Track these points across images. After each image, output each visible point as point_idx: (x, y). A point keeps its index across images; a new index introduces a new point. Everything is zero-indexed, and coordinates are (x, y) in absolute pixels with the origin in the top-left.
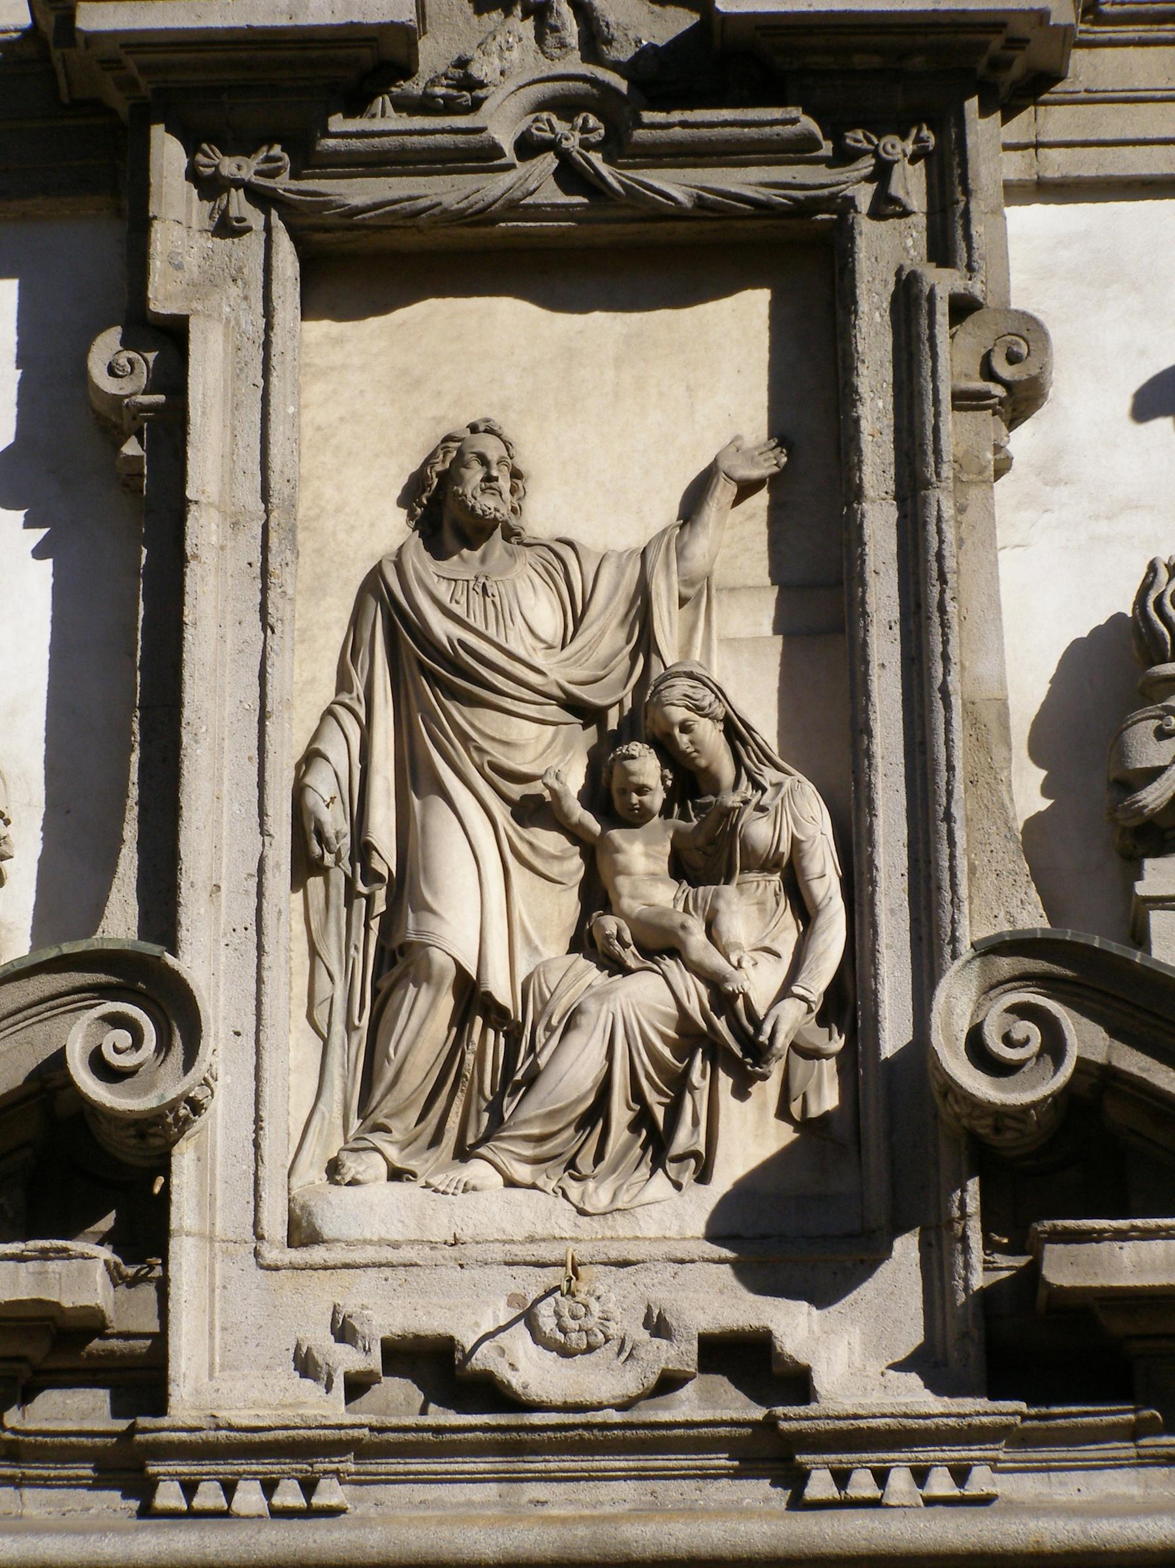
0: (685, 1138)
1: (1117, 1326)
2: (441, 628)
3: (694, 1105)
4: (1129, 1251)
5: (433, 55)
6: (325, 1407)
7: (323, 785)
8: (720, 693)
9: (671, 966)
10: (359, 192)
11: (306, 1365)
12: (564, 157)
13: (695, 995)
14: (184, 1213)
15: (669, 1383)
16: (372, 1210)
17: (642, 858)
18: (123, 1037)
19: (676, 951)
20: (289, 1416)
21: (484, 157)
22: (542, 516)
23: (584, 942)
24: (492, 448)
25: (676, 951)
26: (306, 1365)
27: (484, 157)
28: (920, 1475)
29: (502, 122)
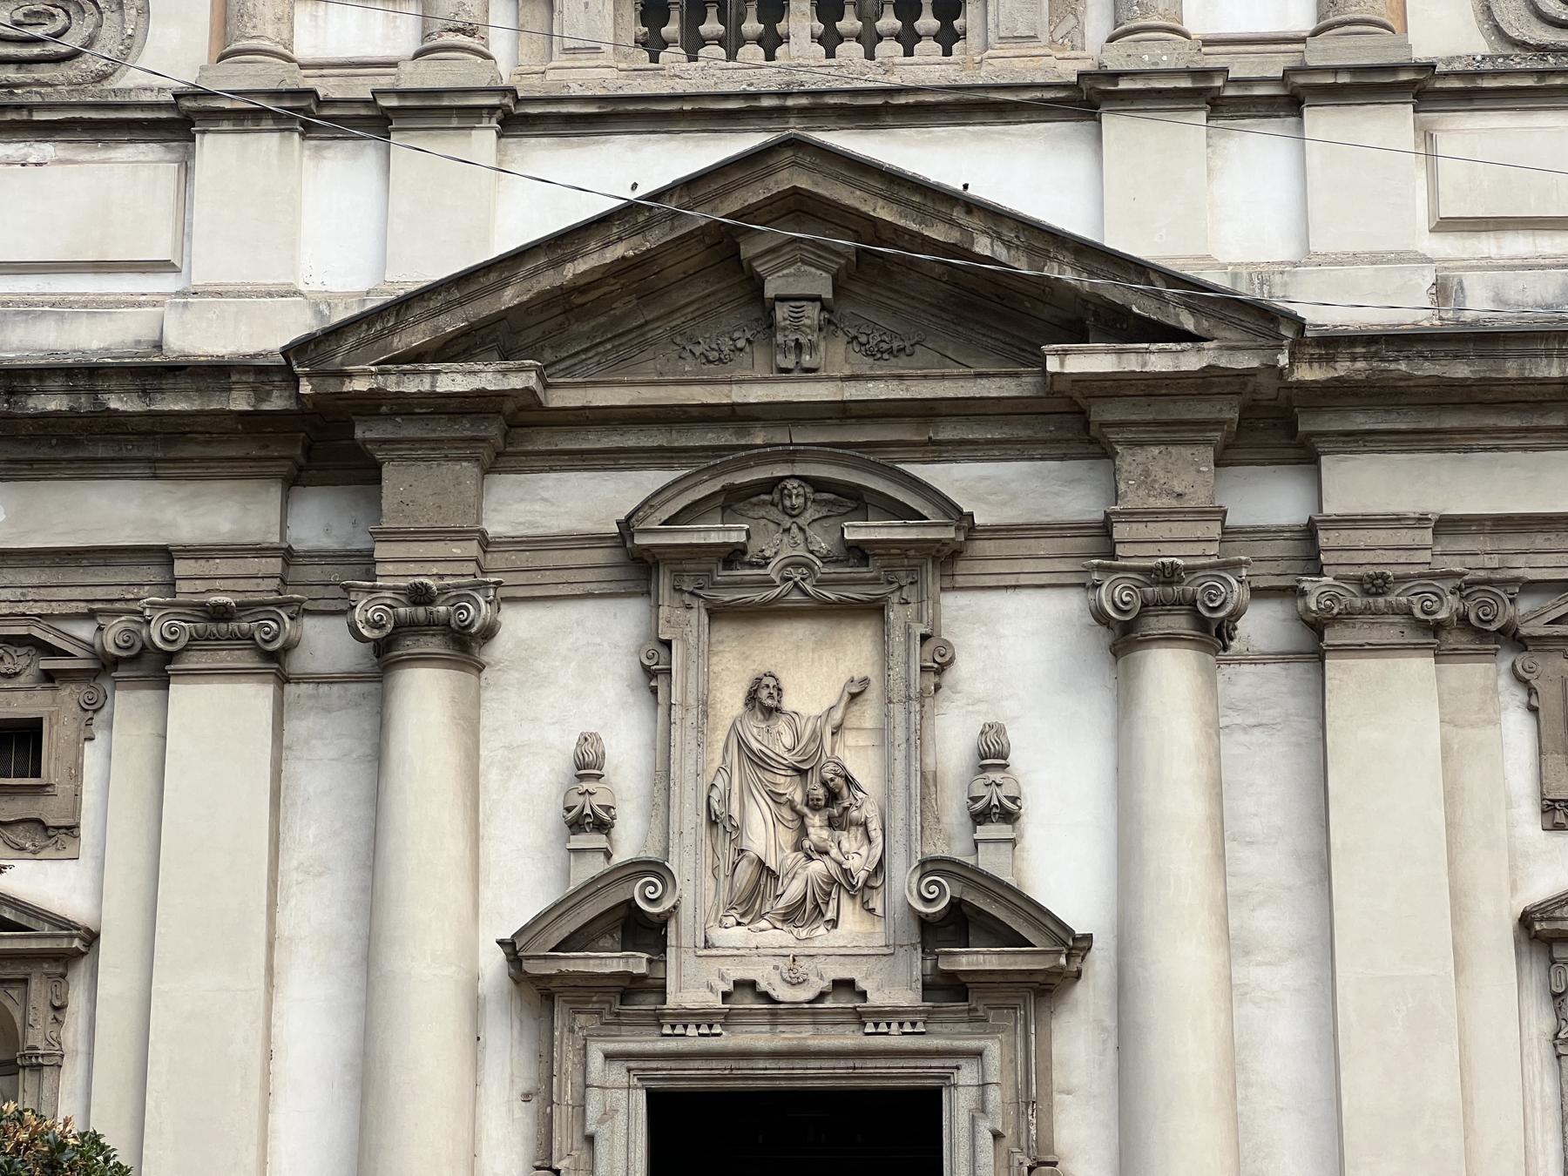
0: (830, 915)
1: (963, 979)
2: (755, 746)
3: (833, 904)
4: (964, 959)
5: (753, 549)
6: (716, 1002)
7: (715, 795)
8: (844, 768)
9: (826, 858)
10: (727, 597)
11: (711, 989)
12: (796, 584)
13: (834, 870)
14: (671, 940)
15: (822, 996)
16: (733, 936)
17: (815, 821)
18: (652, 889)
19: (827, 853)
20: (704, 1005)
21: (770, 584)
22: (788, 703)
23: (798, 847)
24: (772, 682)
25: (827, 853)
26: (711, 989)
27: (770, 584)
28: (901, 1024)
29: (772, 571)
